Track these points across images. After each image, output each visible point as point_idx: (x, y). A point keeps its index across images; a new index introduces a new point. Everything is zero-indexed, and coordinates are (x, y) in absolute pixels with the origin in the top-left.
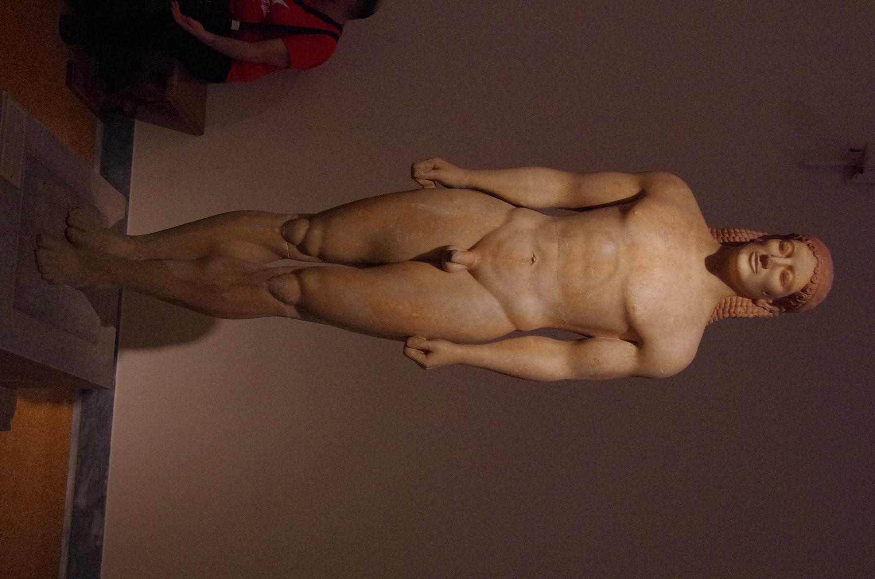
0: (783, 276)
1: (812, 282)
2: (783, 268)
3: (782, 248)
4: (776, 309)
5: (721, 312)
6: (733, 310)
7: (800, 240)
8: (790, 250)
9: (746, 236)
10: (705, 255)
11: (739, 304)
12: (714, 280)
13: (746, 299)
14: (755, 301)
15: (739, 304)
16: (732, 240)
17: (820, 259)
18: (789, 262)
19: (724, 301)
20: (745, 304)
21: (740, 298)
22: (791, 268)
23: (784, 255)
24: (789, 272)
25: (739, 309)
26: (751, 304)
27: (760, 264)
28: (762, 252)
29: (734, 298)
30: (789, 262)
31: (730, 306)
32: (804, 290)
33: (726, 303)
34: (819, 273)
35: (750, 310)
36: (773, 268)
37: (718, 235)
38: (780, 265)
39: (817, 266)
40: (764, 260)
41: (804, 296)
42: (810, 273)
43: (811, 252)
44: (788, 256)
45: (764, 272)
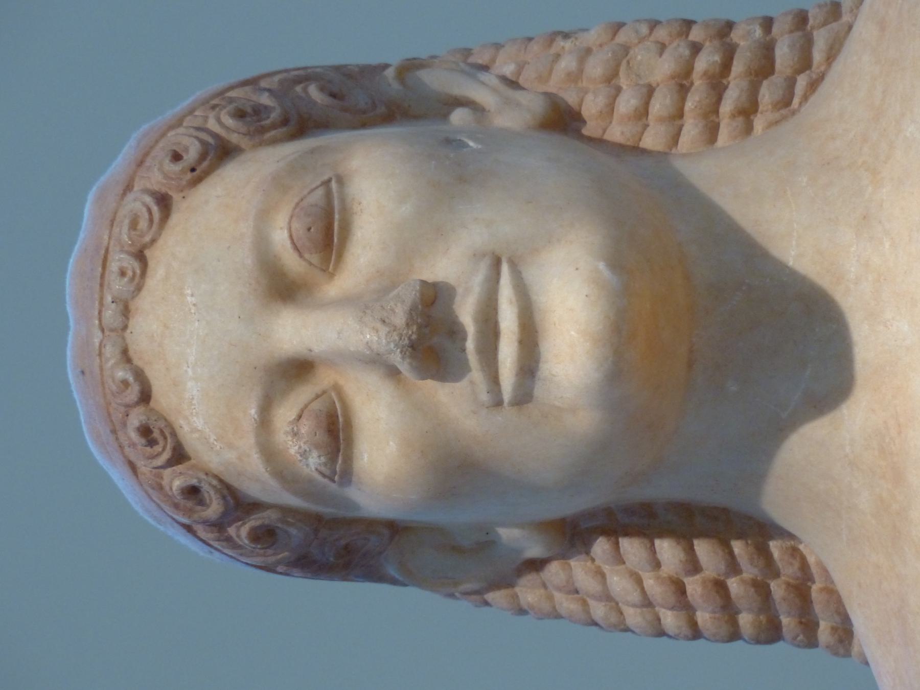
0: (328, 235)
1: (164, 202)
2: (334, 288)
3: (336, 432)
4: (437, 80)
5: (784, 54)
6: (705, 62)
7: (239, 504)
8: (284, 414)
9: (618, 583)
10: (856, 418)
11: (660, 105)
12: (799, 234)
13: (617, 133)
14: (562, 120)
15: (660, 105)
16: (703, 549)
17: (111, 352)
18: (294, 331)
19: (759, 123)
20: (627, 103)
21: (652, 140)
22: (282, 289)
23: (324, 379)
24: (292, 263)
25: (662, 68)
26: (591, 107)
27: (466, 314)
28: (456, 402)
29: (691, 129)
30: (294, 331)
31: (717, 84)
32: (221, 152)
33: (748, 111)
34: (120, 260)
35: (596, 68)
36: (386, 283)
37: (801, 591)
38: (346, 301)
39: (126, 312)
40: (431, 339)
41: (224, 124)
42: (173, 251)
43: (164, 398)
44: (298, 369)
45: (447, 265)
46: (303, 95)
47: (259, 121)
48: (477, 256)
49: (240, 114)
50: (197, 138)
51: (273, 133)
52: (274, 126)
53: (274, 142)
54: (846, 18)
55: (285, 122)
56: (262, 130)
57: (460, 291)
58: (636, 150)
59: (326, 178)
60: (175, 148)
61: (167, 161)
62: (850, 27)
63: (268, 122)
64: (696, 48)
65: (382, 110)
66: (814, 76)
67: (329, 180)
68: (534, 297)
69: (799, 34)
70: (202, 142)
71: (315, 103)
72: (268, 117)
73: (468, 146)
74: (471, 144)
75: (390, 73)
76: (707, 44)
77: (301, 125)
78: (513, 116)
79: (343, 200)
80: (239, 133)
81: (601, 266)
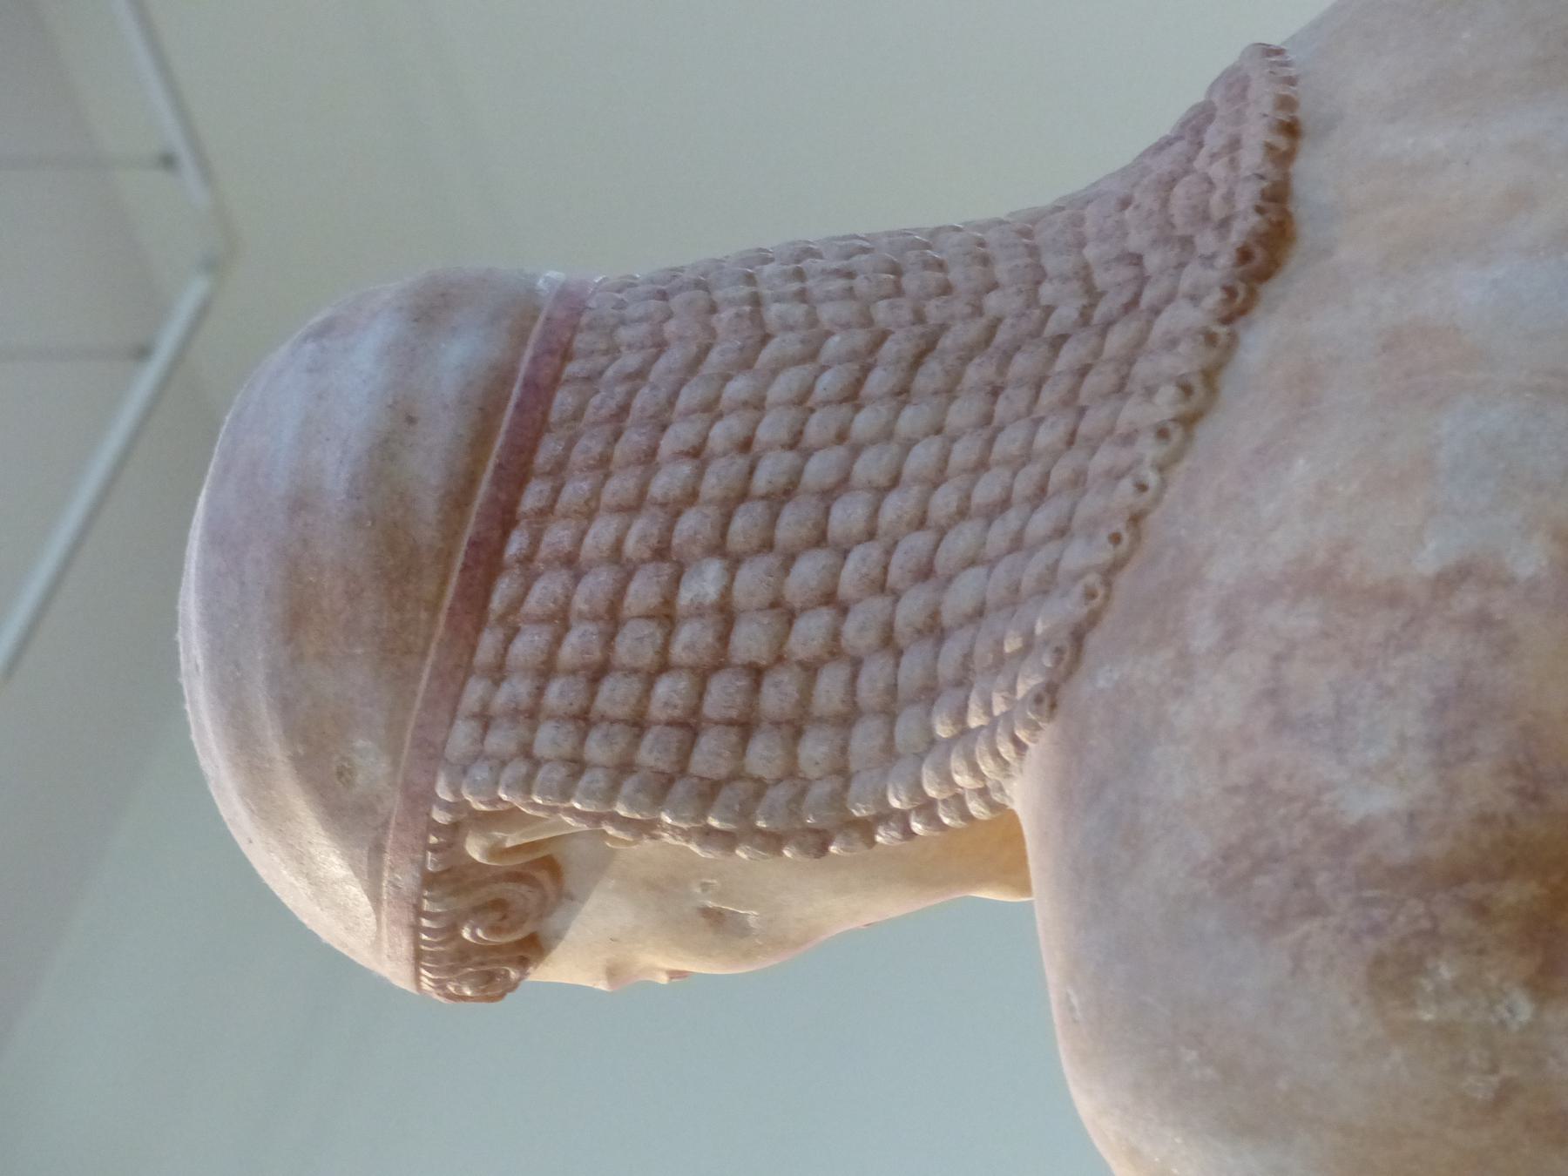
65: (543, 876)
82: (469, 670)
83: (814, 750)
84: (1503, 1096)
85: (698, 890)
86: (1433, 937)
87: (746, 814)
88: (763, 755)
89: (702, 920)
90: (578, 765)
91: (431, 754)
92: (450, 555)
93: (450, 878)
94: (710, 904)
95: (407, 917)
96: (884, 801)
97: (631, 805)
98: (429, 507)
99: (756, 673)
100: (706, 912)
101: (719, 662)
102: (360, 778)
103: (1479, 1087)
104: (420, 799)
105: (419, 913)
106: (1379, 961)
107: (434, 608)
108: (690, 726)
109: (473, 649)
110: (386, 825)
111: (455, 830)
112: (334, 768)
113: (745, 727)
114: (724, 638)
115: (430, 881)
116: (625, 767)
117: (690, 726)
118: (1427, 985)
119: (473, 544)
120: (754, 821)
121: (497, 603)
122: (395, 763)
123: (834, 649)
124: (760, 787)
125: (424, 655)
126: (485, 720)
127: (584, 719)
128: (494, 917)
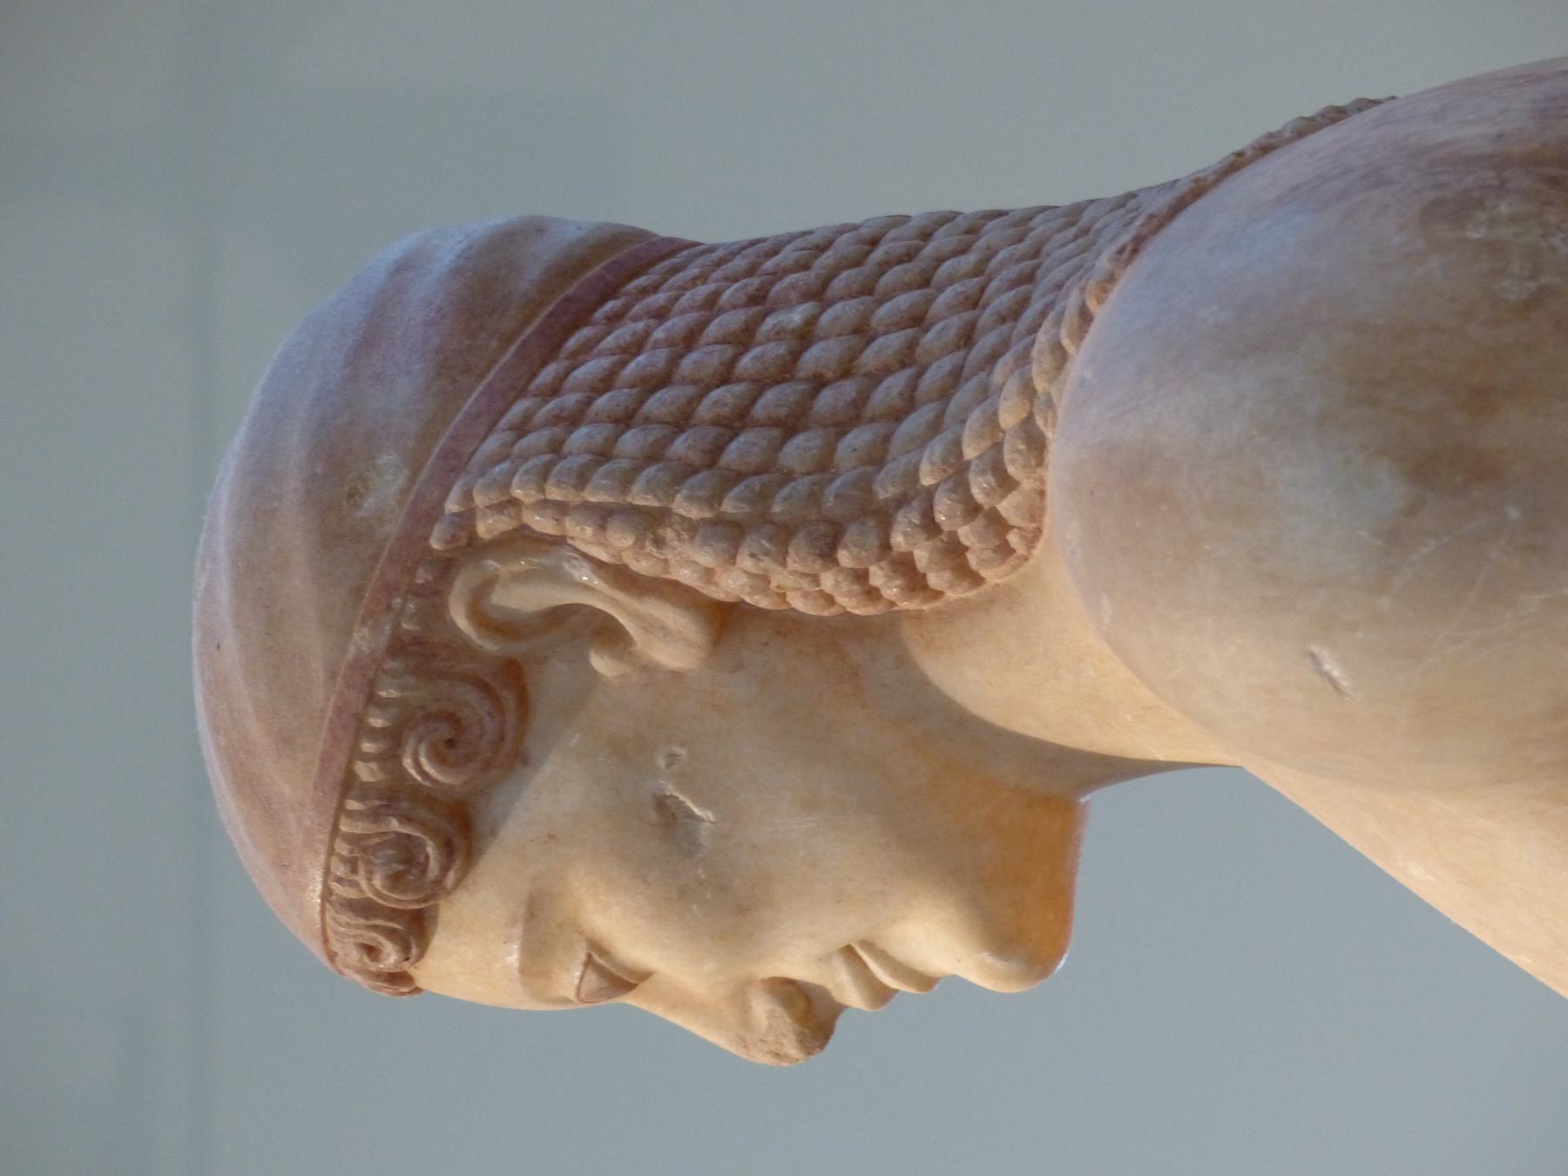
4: (523, 597)
46: (428, 784)
47: (424, 871)
48: (825, 959)
49: (395, 880)
50: (375, 928)
51: (451, 878)
52: (445, 870)
53: (459, 882)
54: (1027, 485)
55: (448, 848)
56: (439, 882)
57: (830, 986)
58: (853, 627)
59: (582, 957)
60: (360, 940)
61: (366, 959)
62: (1042, 494)
63: (434, 868)
64: (861, 576)
65: (509, 698)
66: (1030, 536)
67: (589, 956)
68: (921, 969)
69: (979, 522)
70: (391, 934)
71: (451, 787)
72: (427, 857)
73: (691, 816)
74: (697, 811)
75: (460, 618)
76: (873, 569)
77: (461, 831)
78: (670, 643)
79: (624, 968)
80: (418, 902)
81: (988, 958)
82: (521, 393)
83: (859, 438)
84: (1535, 301)
85: (661, 762)
86: (1501, 189)
87: (763, 497)
88: (799, 450)
89: (653, 816)
90: (603, 455)
91: (454, 465)
92: (541, 305)
93: (422, 651)
94: (670, 789)
95: (356, 699)
96: (912, 475)
97: (650, 487)
98: (534, 271)
99: (819, 383)
100: (661, 802)
101: (784, 372)
102: (369, 503)
103: (1514, 289)
104: (425, 515)
105: (372, 699)
106: (1437, 203)
107: (507, 340)
108: (736, 422)
109: (534, 375)
110: (375, 558)
111: (446, 567)
112: (346, 489)
113: (789, 426)
114: (796, 355)
115: (398, 647)
116: (653, 456)
117: (736, 422)
118: (1482, 216)
119: (567, 300)
120: (770, 507)
121: (572, 343)
122: (412, 479)
123: (907, 358)
124: (788, 476)
125: (482, 376)
126: (521, 429)
127: (625, 420)
128: (445, 731)
